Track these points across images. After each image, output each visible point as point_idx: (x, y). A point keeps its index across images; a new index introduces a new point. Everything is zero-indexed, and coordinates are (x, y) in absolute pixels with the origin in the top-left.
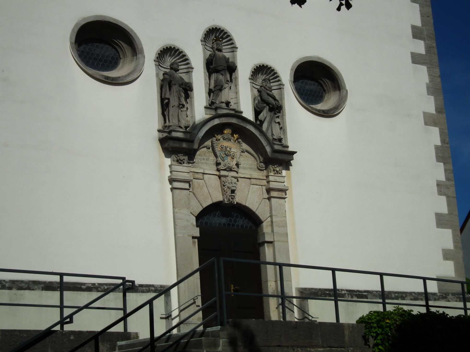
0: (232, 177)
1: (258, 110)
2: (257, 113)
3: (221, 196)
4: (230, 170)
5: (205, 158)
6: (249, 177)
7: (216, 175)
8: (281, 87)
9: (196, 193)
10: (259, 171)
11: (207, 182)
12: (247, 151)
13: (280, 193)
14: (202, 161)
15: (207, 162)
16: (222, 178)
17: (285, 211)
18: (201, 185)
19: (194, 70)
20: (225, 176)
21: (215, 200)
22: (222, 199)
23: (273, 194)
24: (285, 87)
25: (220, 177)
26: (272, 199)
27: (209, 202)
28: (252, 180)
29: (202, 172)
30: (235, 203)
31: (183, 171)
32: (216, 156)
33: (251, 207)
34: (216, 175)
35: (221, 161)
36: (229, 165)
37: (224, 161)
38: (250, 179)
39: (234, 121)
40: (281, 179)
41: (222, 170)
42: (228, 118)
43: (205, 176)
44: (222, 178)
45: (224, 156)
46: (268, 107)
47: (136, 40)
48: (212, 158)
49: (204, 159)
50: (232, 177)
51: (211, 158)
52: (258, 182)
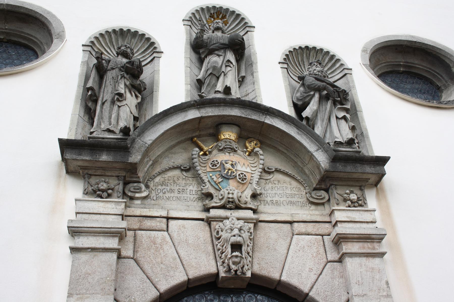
0: (238, 219)
1: (300, 103)
2: (299, 108)
3: (213, 263)
4: (236, 206)
5: (176, 188)
6: (289, 219)
7: (202, 220)
8: (346, 73)
9: (142, 261)
10: (313, 207)
11: (175, 235)
12: (277, 171)
13: (366, 245)
14: (167, 195)
15: (179, 195)
16: (214, 223)
17: (387, 283)
18: (159, 241)
19: (163, 55)
20: (221, 219)
21: (194, 273)
22: (213, 270)
23: (348, 247)
24: (353, 72)
25: (209, 221)
26: (348, 261)
27: (179, 278)
28: (296, 225)
29: (164, 214)
30: (249, 274)
31: (107, 212)
32: (201, 181)
33: (295, 281)
34: (202, 220)
35: (212, 191)
36: (230, 196)
37: (219, 190)
38: (291, 223)
39: (235, 112)
40: (367, 217)
41: (213, 208)
42: (221, 108)
43: (172, 222)
44: (213, 224)
45: (220, 180)
46: (317, 96)
47: (38, 11)
48: (193, 188)
49: (172, 191)
50: (238, 219)
51: (191, 188)
52: (310, 228)
